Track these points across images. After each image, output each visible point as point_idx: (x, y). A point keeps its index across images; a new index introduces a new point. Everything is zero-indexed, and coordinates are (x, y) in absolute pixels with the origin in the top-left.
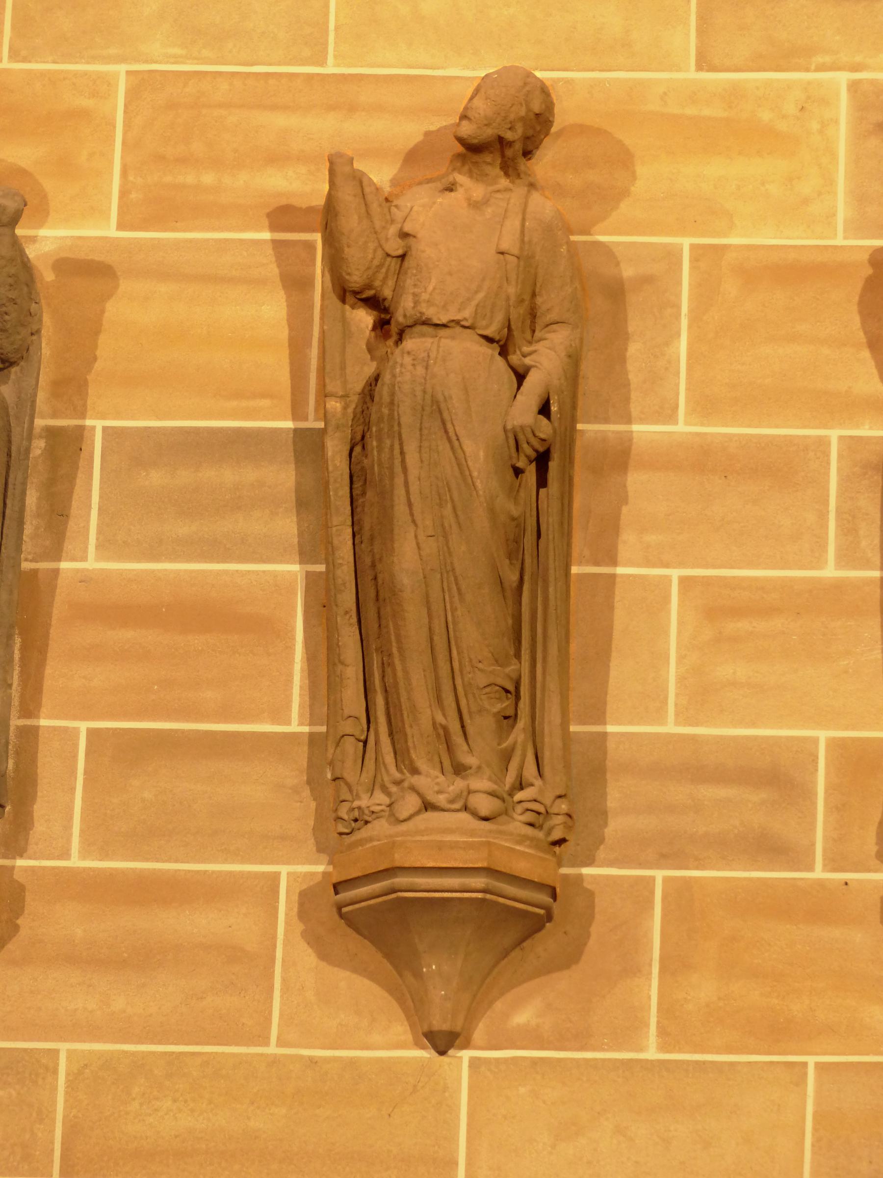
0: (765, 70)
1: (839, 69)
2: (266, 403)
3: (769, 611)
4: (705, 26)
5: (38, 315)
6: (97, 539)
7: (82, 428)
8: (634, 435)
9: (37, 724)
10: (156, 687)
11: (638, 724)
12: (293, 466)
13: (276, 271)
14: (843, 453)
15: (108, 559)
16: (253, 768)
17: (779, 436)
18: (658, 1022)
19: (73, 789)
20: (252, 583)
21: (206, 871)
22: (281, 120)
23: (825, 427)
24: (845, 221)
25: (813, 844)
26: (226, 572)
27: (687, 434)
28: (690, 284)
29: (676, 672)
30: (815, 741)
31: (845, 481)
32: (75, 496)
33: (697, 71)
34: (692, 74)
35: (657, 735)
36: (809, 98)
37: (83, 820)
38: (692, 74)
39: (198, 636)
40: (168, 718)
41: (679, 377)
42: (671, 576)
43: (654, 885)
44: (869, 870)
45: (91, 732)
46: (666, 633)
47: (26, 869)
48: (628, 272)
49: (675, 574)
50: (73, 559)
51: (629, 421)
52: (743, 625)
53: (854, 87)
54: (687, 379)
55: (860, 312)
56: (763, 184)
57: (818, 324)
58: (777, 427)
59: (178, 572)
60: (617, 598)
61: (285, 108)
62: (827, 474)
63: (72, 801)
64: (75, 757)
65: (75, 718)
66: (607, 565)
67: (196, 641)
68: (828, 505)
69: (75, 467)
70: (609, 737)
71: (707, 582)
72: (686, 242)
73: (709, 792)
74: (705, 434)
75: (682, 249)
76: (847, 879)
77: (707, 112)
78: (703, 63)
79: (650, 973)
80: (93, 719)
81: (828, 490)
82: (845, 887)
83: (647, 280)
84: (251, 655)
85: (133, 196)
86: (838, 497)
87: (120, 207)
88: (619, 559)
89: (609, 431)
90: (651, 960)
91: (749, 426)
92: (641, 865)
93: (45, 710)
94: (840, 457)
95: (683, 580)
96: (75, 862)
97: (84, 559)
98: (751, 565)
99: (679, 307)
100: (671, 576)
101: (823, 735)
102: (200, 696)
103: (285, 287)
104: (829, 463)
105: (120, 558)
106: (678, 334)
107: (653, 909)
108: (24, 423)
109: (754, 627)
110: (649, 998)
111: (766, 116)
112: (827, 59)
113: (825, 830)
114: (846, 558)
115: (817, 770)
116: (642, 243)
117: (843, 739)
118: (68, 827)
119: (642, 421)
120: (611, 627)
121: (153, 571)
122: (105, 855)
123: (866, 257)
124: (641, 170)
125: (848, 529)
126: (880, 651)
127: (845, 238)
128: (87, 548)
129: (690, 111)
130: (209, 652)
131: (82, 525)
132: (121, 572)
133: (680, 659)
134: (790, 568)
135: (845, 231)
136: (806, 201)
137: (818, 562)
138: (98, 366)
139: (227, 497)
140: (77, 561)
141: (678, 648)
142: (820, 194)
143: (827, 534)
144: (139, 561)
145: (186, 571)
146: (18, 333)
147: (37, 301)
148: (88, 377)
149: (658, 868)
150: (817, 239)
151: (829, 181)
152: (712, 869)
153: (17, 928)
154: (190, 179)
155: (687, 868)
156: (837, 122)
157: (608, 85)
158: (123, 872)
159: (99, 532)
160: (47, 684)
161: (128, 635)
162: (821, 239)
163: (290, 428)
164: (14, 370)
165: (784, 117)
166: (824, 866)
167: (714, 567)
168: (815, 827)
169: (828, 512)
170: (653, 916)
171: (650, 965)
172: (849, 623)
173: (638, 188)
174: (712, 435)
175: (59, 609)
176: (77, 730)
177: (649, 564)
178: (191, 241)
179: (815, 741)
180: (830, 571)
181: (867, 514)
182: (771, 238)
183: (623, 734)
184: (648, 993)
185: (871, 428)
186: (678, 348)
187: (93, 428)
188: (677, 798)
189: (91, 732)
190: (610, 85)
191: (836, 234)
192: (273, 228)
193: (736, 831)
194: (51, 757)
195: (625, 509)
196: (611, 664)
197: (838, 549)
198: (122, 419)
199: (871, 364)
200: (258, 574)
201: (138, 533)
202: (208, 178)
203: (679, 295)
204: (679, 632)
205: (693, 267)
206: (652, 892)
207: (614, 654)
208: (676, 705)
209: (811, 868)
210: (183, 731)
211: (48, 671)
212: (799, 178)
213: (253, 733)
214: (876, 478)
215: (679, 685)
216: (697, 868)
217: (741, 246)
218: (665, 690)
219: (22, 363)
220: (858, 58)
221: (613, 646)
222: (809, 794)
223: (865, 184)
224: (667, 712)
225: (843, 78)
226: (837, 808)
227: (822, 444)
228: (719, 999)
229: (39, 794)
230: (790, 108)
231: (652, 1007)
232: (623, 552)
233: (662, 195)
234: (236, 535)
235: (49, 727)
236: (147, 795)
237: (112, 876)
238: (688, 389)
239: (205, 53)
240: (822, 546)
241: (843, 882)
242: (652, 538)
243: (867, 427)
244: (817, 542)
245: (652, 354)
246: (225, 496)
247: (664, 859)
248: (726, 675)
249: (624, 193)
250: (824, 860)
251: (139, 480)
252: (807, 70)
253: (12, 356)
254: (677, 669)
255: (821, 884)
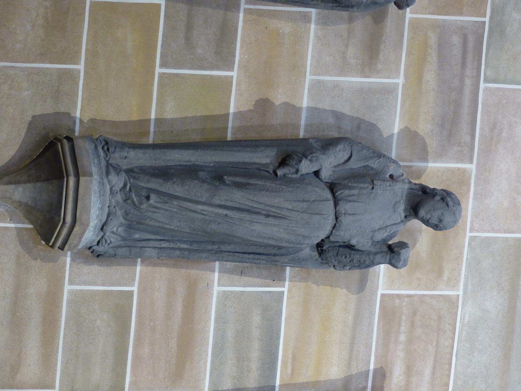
2: (289, 371)
5: (343, 270)
6: (228, 291)
7: (284, 280)
9: (138, 265)
10: (152, 324)
12: (257, 386)
13: (354, 373)
15: (218, 297)
16: (108, 374)
19: (103, 285)
20: (201, 368)
21: (58, 353)
22: (427, 372)
26: (207, 355)
32: (250, 279)
37: (88, 291)
39: (176, 343)
40: (137, 331)
45: (132, 292)
47: (65, 263)
50: (219, 279)
59: (209, 332)
61: (433, 373)
63: (98, 285)
64: (120, 285)
65: (140, 284)
67: (173, 342)
69: (266, 278)
80: (139, 293)
84: (165, 369)
85: (397, 301)
87: (392, 295)
93: (144, 269)
96: (67, 288)
97: (219, 285)
102: (146, 345)
103: (345, 377)
105: (218, 303)
108: (290, 264)
118: (85, 283)
121: (210, 320)
122: (69, 303)
128: (224, 286)
130: (168, 349)
131: (236, 283)
132: (211, 304)
138: (315, 286)
139: (244, 354)
140: (218, 281)
144: (216, 312)
145: (209, 336)
146: (335, 261)
147: (350, 269)
148: (309, 282)
153: (36, 259)
154: (403, 328)
158: (60, 312)
159: (232, 292)
160: (157, 269)
161: (179, 308)
163: (276, 384)
164: (316, 254)
175: (194, 272)
176: (133, 285)
178: (373, 331)
187: (284, 287)
189: (131, 293)
192: (375, 371)
194: (121, 274)
198: (287, 300)
200: (204, 371)
201: (230, 311)
202: (402, 338)
210: (129, 338)
211: (164, 269)
213: (125, 373)
219: (320, 259)
229: (103, 268)
234: (225, 360)
235: (136, 271)
236: (99, 322)
237: (59, 306)
239: (464, 333)
246: (245, 354)
251: (256, 310)
253: (324, 256)
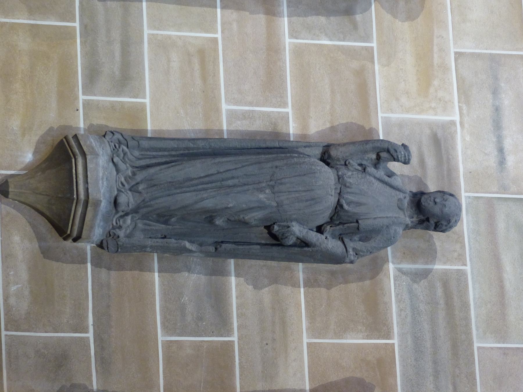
0: (457, 83)
1: (461, 117)
3: (204, 79)
4: (476, 56)
8: (283, 19)
11: (147, 17)
14: (281, 114)
17: (287, 85)
18: (7, 23)
23: (292, 106)
24: (390, 117)
25: (95, 95)
27: (285, 43)
28: (355, 46)
29: (173, 35)
30: (144, 98)
31: (268, 114)
33: (454, 52)
34: (452, 50)
35: (142, 26)
36: (446, 102)
38: (452, 50)
41: (311, 40)
42: (218, 34)
43: (72, 22)
44: (84, 120)
46: (191, 31)
48: (358, 17)
49: (219, 36)
51: (288, 16)
52: (197, 66)
53: (453, 123)
54: (310, 43)
55: (347, 123)
56: (404, 80)
57: (341, 104)
58: (291, 84)
60: (205, 9)
62: (270, 106)
66: (221, 5)
68: (255, 106)
70: (140, 3)
71: (216, 50)
72: (374, 45)
73: (117, 48)
74: (285, 51)
75: (371, 43)
76: (79, 111)
77: (436, 56)
78: (458, 55)
79: (30, 19)
81: (262, 107)
82: (76, 110)
83: (355, 27)
86: (260, 111)
88: (224, 10)
89: (284, 8)
90: (36, 20)
91: (290, 71)
92: (81, 16)
94: (279, 113)
95: (215, 40)
98: (225, 71)
99: (344, 40)
100: (218, 34)
101: (147, 101)
104: (275, 107)
106: (331, 40)
107: (61, 22)
109: (196, 71)
110: (18, 19)
111: (436, 83)
112: (465, 112)
113: (102, 101)
114: (232, 115)
115: (130, 98)
116: (372, 25)
117: (146, 110)
119: (290, 22)
120: (192, 6)
123: (374, 126)
124: (406, 24)
125: (245, 116)
126: (188, 128)
127: (382, 117)
129: (436, 49)
133: (180, 37)
134: (225, 88)
135: (385, 117)
136: (397, 99)
137: (228, 102)
141: (184, 36)
142: (402, 106)
143: (242, 106)
149: (80, 24)
150: (380, 104)
151: (408, 111)
152: (81, 49)
155: (81, 37)
156: (436, 115)
157: (444, 12)
162: (380, 106)
165: (436, 91)
166: (85, 100)
167: (223, 54)
168: (103, 96)
169: (253, 107)
170: (58, 21)
171: (34, 20)
172: (201, 115)
173: (398, 23)
174: (285, 54)
177: (223, 24)
179: (144, 98)
180: (225, 107)
181: (253, 124)
182: (379, 83)
183: (142, 10)
184: (20, 18)
185: (293, 127)
186: (325, 40)
188: (113, 34)
190: (445, 13)
191: (383, 113)
193: (99, 60)
195: (247, 13)
196: (174, 5)
197: (235, 111)
199: (324, 128)
203: (349, 41)
204: (192, 37)
205: (362, 48)
206: (68, 21)
207: (179, 7)
208: (157, 34)
209: (84, 94)
212: (408, 97)
214: (270, 129)
215: (167, 36)
216: (81, 42)
217: (374, 69)
218: (164, 30)
220: (466, 125)
221: (183, 7)
222: (119, 94)
223: (408, 127)
224: (154, 30)
225: (457, 118)
226: (113, 106)
227: (285, 105)
228: (20, 51)
230: (440, 94)
231: (14, 20)
232: (228, 12)
233: (395, 35)
238: (306, 44)
240: (236, 103)
241: (78, 109)
242: (235, 26)
243: (294, 125)
244: (238, 101)
245: (321, 28)
247: (84, 27)
248: (173, 58)
249: (395, 17)
250: (88, 100)
252: (459, 102)
254: (174, 35)
255: (77, 98)
